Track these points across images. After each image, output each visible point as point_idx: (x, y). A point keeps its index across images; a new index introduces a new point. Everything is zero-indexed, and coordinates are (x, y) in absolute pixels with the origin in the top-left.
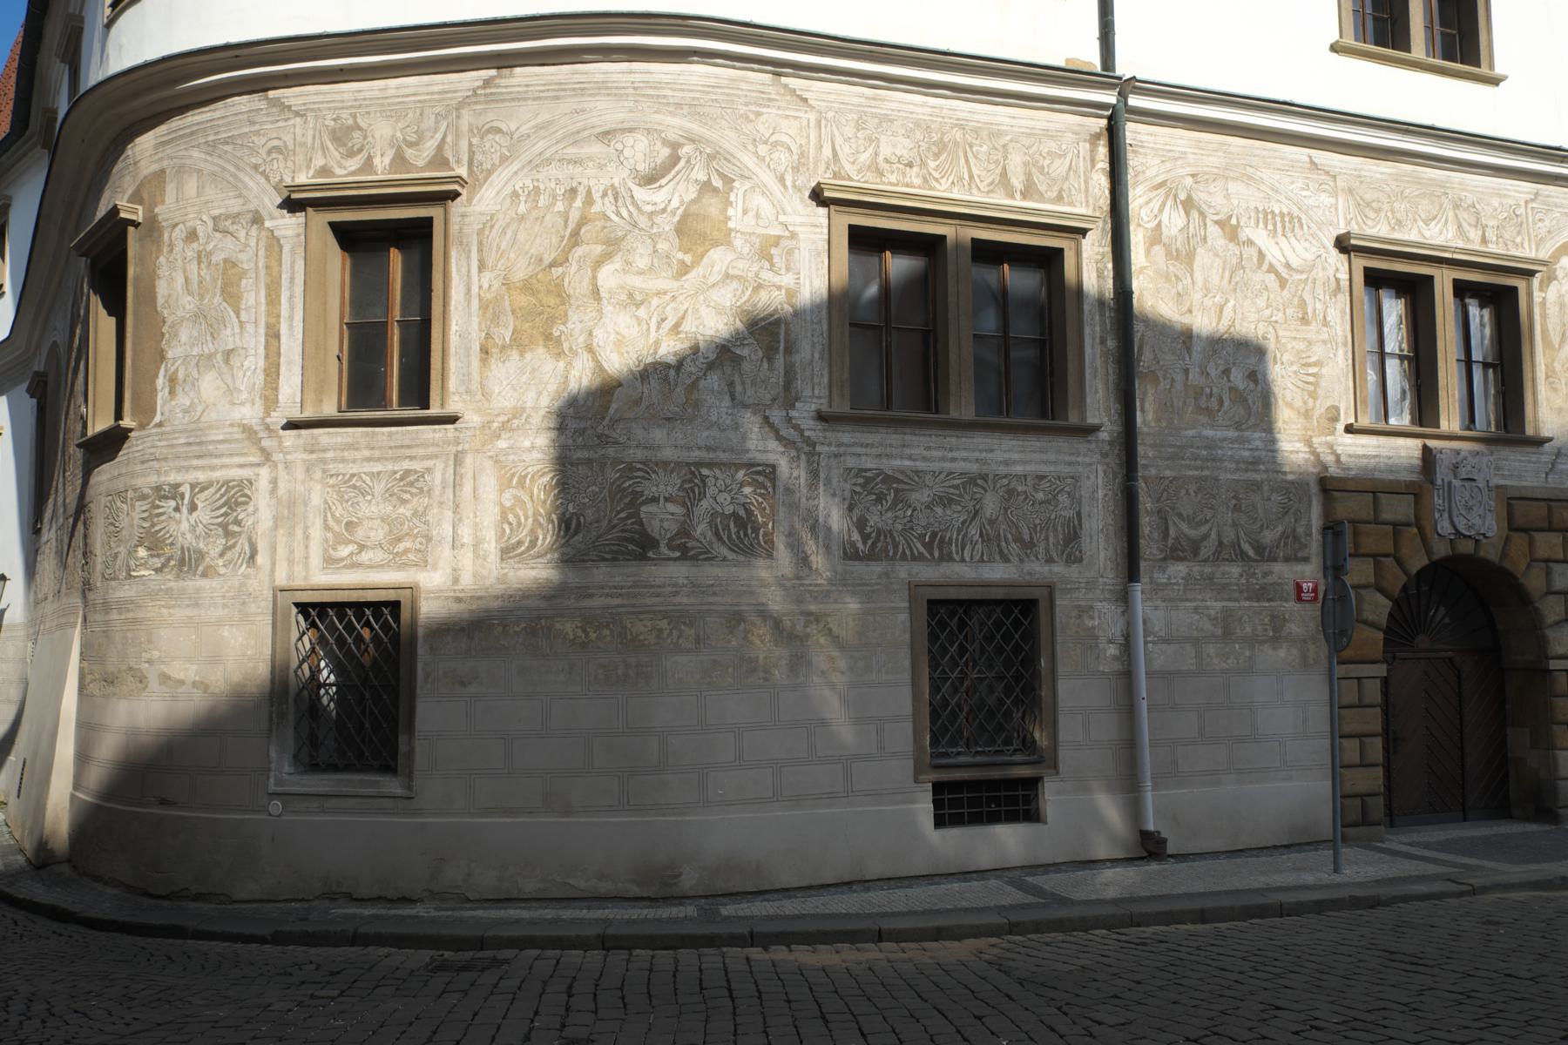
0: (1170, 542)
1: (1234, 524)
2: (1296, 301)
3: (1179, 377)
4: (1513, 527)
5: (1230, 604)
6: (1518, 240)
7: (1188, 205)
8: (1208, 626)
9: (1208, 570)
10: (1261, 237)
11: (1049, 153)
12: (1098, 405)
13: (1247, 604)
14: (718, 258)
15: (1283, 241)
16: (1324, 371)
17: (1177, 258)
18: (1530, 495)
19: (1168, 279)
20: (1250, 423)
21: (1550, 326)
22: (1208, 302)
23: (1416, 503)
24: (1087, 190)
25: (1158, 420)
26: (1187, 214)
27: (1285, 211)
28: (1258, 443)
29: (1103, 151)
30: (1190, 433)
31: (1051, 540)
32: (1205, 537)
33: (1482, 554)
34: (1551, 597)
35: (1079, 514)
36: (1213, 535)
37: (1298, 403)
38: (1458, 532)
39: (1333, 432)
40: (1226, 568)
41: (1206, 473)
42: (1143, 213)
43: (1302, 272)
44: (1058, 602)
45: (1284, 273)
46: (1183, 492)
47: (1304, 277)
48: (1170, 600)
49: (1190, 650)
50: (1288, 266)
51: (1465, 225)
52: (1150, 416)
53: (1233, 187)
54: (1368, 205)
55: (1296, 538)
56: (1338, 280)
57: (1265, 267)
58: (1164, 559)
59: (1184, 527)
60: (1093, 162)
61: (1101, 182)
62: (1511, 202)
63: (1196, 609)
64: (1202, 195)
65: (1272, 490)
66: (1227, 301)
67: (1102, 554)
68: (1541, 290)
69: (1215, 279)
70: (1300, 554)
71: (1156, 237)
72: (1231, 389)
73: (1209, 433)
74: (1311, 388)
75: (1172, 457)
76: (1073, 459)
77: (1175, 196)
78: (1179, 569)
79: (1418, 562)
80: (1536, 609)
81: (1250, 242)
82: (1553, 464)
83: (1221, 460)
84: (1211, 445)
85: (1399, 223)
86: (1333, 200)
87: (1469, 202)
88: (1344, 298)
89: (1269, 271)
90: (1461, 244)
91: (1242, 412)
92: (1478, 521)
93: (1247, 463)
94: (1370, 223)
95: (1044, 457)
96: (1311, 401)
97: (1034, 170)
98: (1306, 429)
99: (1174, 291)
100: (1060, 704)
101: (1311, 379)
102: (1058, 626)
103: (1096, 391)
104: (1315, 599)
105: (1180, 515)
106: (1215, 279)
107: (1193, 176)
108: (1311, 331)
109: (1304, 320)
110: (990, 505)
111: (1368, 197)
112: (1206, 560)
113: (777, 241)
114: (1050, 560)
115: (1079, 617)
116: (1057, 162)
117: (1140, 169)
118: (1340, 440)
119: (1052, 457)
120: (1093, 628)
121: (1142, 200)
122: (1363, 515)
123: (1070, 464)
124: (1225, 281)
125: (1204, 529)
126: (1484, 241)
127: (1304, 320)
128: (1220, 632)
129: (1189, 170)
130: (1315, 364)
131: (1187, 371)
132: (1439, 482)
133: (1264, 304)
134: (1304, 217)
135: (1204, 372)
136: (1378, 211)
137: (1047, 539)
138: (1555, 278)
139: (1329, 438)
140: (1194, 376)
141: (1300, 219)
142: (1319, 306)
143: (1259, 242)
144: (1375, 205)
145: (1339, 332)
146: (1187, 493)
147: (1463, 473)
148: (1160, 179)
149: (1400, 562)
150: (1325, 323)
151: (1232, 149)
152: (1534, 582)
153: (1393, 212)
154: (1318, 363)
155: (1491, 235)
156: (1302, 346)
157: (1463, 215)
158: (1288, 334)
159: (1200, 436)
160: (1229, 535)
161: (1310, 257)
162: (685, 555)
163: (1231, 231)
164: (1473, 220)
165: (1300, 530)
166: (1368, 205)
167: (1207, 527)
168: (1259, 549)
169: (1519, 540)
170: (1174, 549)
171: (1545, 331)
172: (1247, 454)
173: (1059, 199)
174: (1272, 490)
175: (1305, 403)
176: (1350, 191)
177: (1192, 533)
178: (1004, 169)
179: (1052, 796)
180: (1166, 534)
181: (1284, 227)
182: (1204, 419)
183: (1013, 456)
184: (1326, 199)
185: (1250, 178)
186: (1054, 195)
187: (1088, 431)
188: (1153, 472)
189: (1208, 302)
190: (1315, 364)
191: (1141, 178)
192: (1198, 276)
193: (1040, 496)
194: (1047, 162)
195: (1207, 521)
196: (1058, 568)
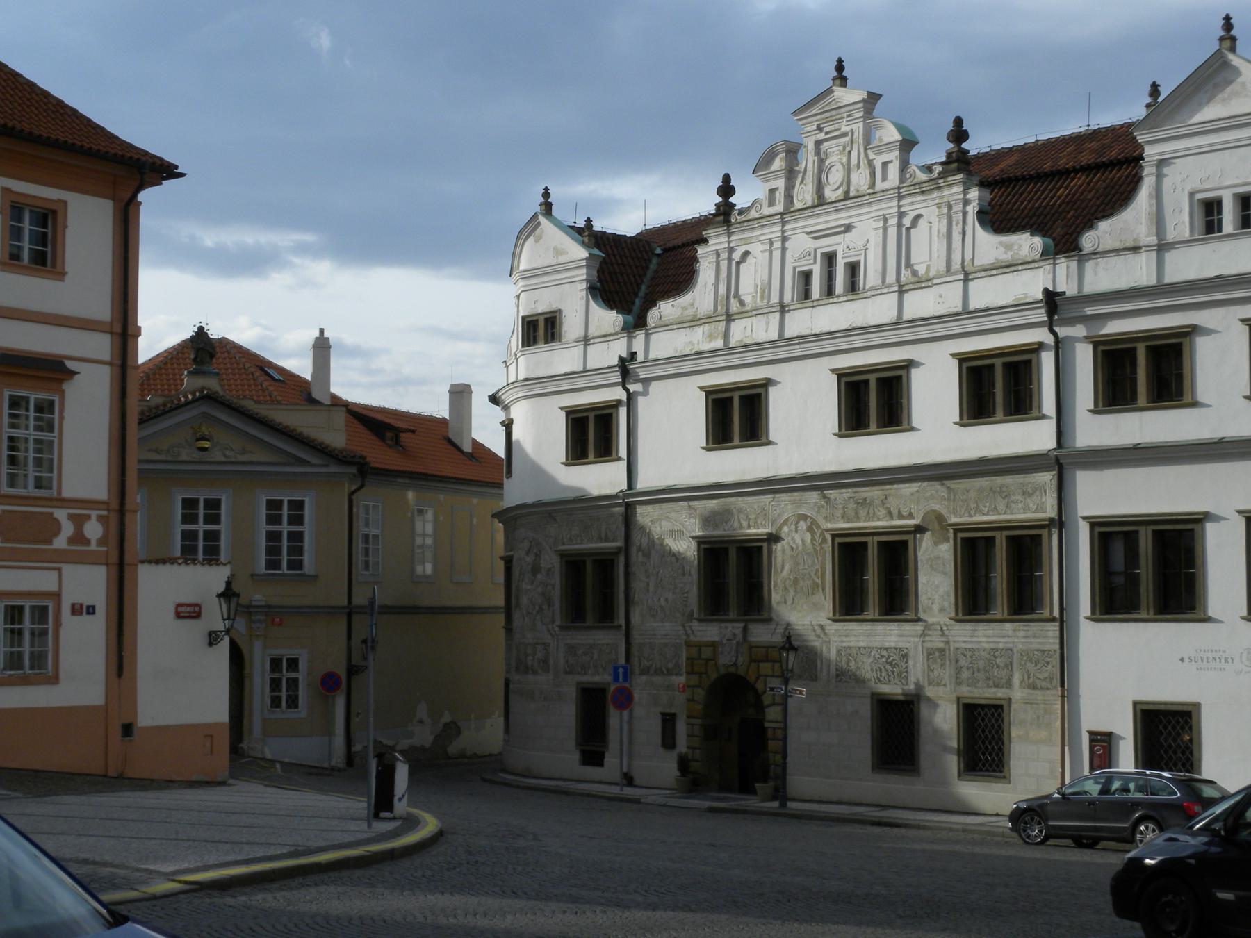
4: (752, 661)
14: (539, 576)
78: (644, 678)
79: (714, 676)
110: (596, 656)
113: (549, 570)
127: (684, 574)
152: (759, 686)
155: (752, 523)
162: (535, 673)
168: (668, 670)
169: (753, 665)
173: (613, 541)
179: (608, 760)
183: (603, 637)
184: (693, 520)
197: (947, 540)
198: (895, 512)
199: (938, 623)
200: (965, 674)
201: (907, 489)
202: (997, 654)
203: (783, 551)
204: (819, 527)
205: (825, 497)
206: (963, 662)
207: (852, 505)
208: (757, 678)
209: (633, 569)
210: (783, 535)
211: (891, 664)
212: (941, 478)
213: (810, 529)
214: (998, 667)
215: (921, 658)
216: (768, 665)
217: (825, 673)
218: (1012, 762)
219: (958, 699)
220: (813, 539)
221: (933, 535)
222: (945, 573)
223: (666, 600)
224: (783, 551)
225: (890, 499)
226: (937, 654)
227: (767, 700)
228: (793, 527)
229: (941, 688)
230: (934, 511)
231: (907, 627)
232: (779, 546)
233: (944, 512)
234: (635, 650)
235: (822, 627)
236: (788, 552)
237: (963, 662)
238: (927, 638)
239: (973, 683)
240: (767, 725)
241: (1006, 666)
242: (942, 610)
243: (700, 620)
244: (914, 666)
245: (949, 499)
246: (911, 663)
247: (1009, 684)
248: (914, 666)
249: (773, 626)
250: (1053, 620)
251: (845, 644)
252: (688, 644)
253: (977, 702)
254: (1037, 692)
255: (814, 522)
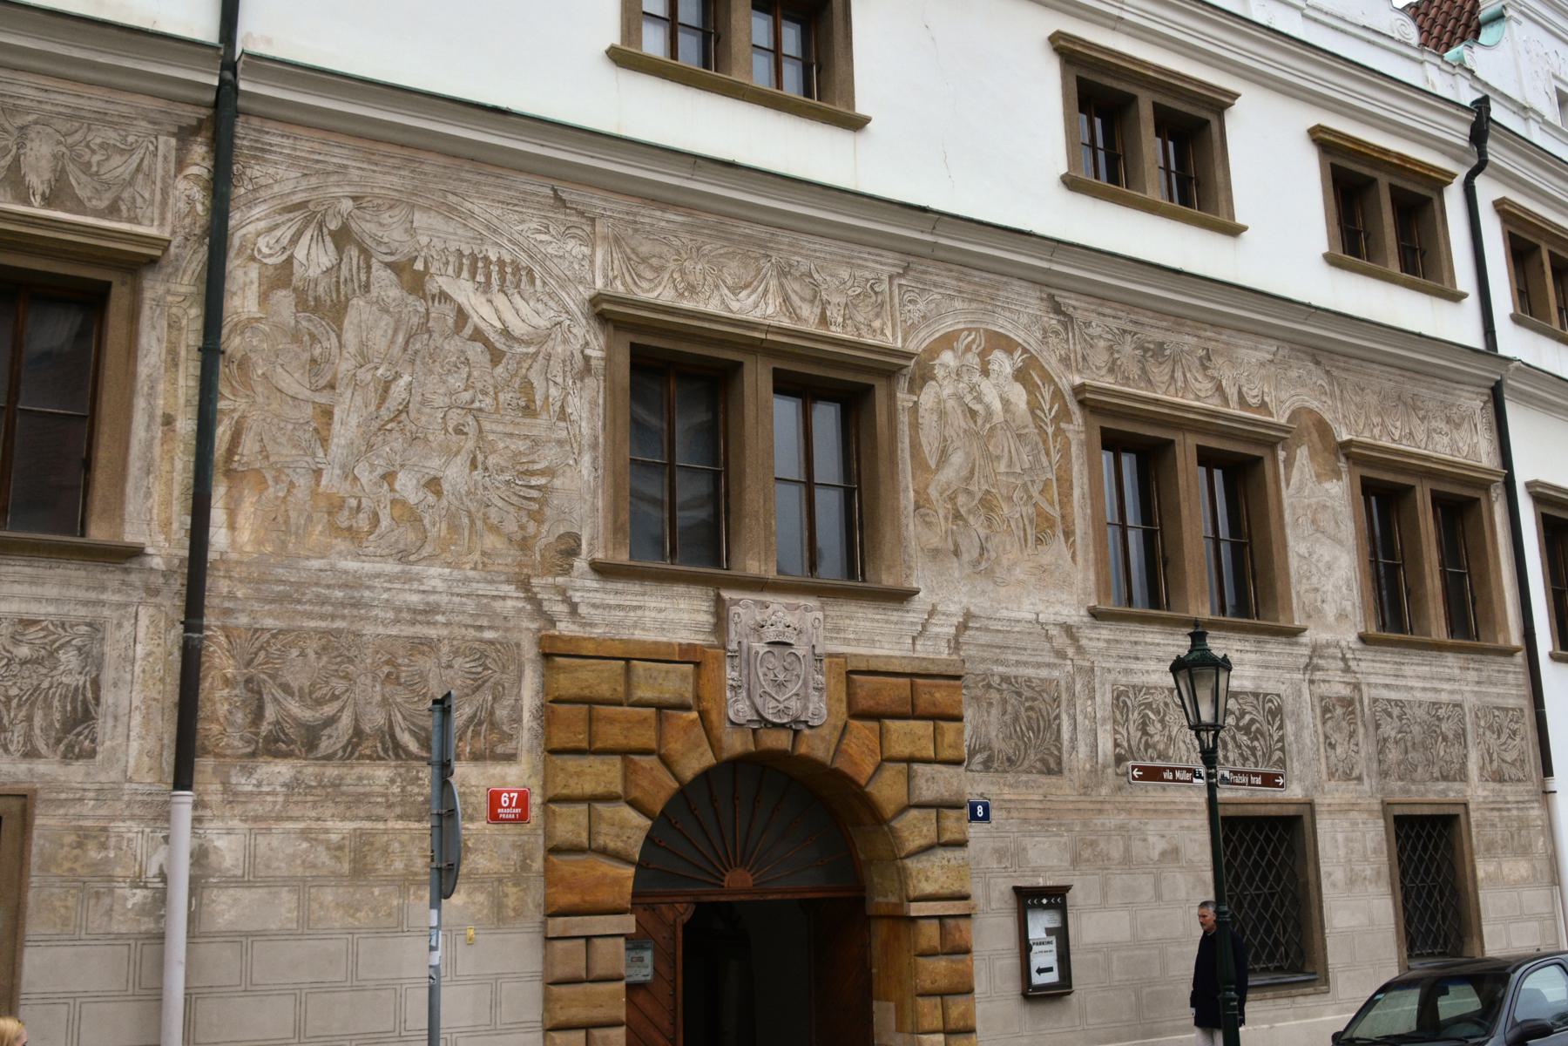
0: (265, 728)
1: (385, 702)
2: (517, 382)
3: (303, 482)
5: (367, 825)
6: (877, 324)
7: (342, 237)
8: (323, 856)
9: (332, 771)
10: (464, 292)
11: (103, 146)
12: (148, 513)
13: (399, 825)
15: (500, 300)
16: (558, 483)
17: (315, 310)
18: (883, 668)
19: (296, 336)
20: (424, 554)
21: (924, 441)
22: (364, 375)
23: (698, 677)
24: (164, 203)
25: (260, 543)
26: (340, 250)
27: (507, 258)
28: (440, 585)
29: (199, 151)
30: (316, 564)
31: (38, 720)
32: (331, 721)
33: (803, 749)
34: (914, 813)
35: (96, 684)
36: (346, 720)
37: (511, 527)
38: (762, 719)
39: (567, 571)
40: (365, 769)
41: (339, 624)
42: (262, 243)
43: (528, 344)
44: (38, 821)
45: (500, 343)
46: (295, 652)
47: (532, 350)
48: (256, 819)
49: (287, 898)
50: (506, 333)
51: (794, 297)
52: (245, 536)
53: (420, 219)
54: (644, 260)
55: (493, 725)
56: (587, 359)
57: (468, 331)
58: (253, 755)
59: (294, 707)
60: (181, 164)
61: (189, 193)
62: (868, 275)
63: (304, 834)
64: (367, 227)
65: (456, 653)
66: (398, 376)
67: (135, 745)
68: (911, 391)
69: (379, 341)
70: (500, 749)
71: (282, 276)
72: (394, 502)
73: (351, 565)
74: (535, 506)
75: (280, 599)
76: (93, 595)
77: (321, 226)
78: (280, 771)
79: (696, 761)
80: (892, 830)
81: (444, 296)
82: (924, 626)
83: (369, 606)
84: (353, 583)
85: (692, 289)
86: (587, 251)
87: (803, 269)
88: (595, 386)
89: (472, 338)
90: (786, 323)
91: (411, 536)
92: (795, 705)
93: (415, 611)
94: (645, 285)
95: (37, 591)
96: (532, 527)
97: (71, 167)
98: (520, 565)
99: (306, 356)
100: (24, 988)
101: (535, 494)
102: (35, 860)
103: (148, 495)
104: (523, 818)
105: (286, 689)
106: (379, 341)
107: (355, 199)
108: (540, 426)
109: (529, 410)
111: (645, 249)
112: (329, 758)
114: (31, 754)
115: (80, 845)
116: (116, 160)
117: (263, 181)
118: (578, 583)
119: (52, 591)
120: (106, 861)
121: (262, 225)
122: (605, 691)
123: (86, 603)
124: (396, 350)
125: (329, 710)
126: (824, 320)
127: (529, 410)
128: (346, 867)
129: (348, 190)
130: (542, 473)
131: (318, 473)
132: (733, 646)
133: (460, 385)
134: (537, 269)
135: (349, 474)
136: (658, 270)
137: (29, 719)
138: (933, 378)
139: (560, 580)
140: (331, 481)
141: (530, 272)
142: (553, 391)
143: (461, 299)
144: (654, 261)
145: (586, 430)
146: (303, 654)
147: (771, 634)
148: (297, 198)
149: (666, 761)
150: (563, 415)
151: (427, 169)
152: (887, 790)
153: (682, 272)
154: (549, 472)
156: (522, 446)
157: (793, 286)
158: (500, 428)
159: (333, 569)
160: (375, 719)
161: (543, 323)
163: (412, 278)
164: (808, 294)
165: (502, 713)
166: (644, 260)
167: (336, 705)
170: (272, 739)
171: (915, 446)
172: (414, 598)
173: (113, 211)
174: (456, 653)
175: (522, 527)
176: (617, 240)
177: (307, 715)
178: (17, 159)
180: (258, 715)
181: (503, 280)
182: (341, 544)
184: (575, 248)
185: (451, 209)
186: (103, 204)
187: (128, 555)
188: (243, 620)
189: (364, 375)
190: (542, 473)
191: (263, 194)
192: (350, 337)
193: (24, 651)
194: (95, 159)
195: (335, 698)
196: (48, 768)
197: (1337, 474)
198: (1232, 392)
199: (1337, 645)
200: (1393, 755)
201: (1253, 354)
202: (1441, 712)
203: (942, 414)
204: (1048, 378)
205: (1057, 309)
206: (1389, 729)
207: (1128, 348)
208: (878, 768)
209: (233, 343)
210: (939, 372)
211: (1246, 730)
212: (1317, 353)
213: (1021, 376)
214: (1445, 739)
215: (1309, 717)
216: (923, 728)
217: (1083, 750)
218: (1487, 929)
219: (1386, 805)
220: (1034, 407)
221: (1312, 456)
222: (1340, 543)
223: (433, 485)
224: (942, 414)
225: (1218, 361)
226: (1339, 711)
227: (915, 829)
228: (973, 360)
229: (1352, 785)
230: (1310, 411)
231: (1276, 649)
232: (927, 397)
233: (1328, 417)
234: (220, 662)
235: (1068, 629)
236: (959, 421)
237: (1389, 729)
238: (1318, 675)
239: (1407, 772)
240: (916, 909)
241: (1457, 736)
242: (1342, 616)
243: (602, 570)
244: (1298, 736)
245: (1332, 395)
246: (1290, 728)
247: (1462, 775)
248: (1298, 736)
249: (914, 614)
250: (1509, 652)
251: (1137, 680)
252: (551, 653)
253: (1418, 811)
254: (1508, 788)
255: (1031, 361)
